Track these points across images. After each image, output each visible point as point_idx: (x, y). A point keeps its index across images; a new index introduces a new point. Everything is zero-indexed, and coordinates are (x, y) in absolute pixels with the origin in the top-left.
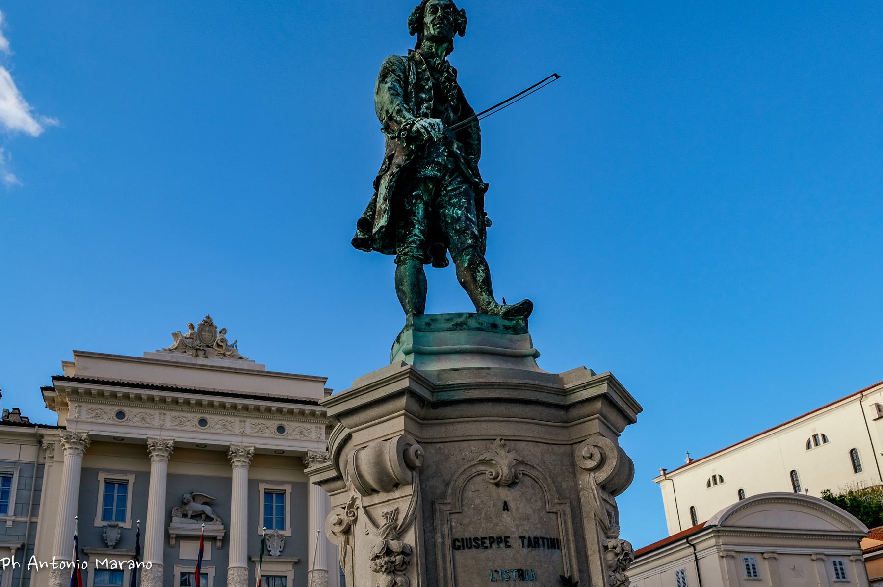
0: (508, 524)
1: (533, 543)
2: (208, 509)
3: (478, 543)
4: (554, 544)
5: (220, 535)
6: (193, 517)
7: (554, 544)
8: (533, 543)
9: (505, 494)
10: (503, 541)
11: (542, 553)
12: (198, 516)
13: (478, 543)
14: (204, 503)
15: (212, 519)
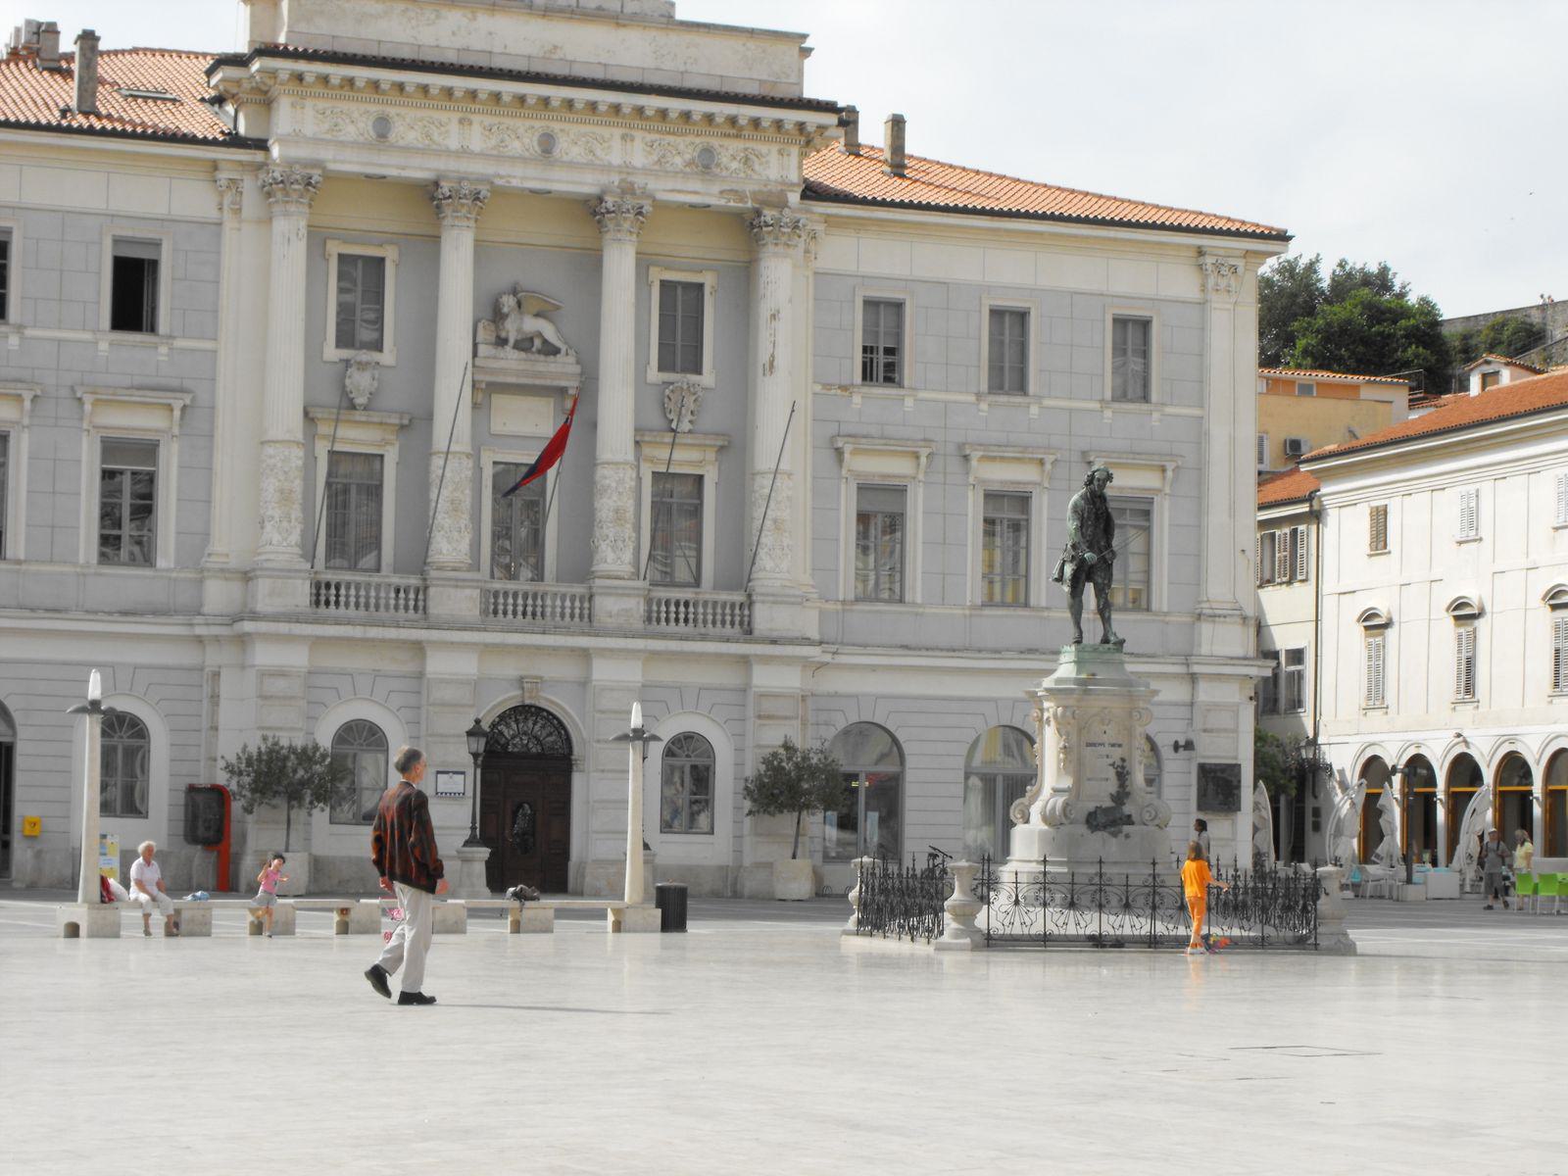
0: (1105, 739)
1: (1113, 745)
2: (549, 332)
3: (1094, 745)
4: (1120, 746)
5: (572, 384)
6: (517, 346)
7: (1120, 746)
8: (1113, 745)
9: (1105, 728)
10: (1102, 744)
11: (1117, 748)
12: (524, 344)
13: (1094, 745)
14: (537, 315)
15: (556, 351)
